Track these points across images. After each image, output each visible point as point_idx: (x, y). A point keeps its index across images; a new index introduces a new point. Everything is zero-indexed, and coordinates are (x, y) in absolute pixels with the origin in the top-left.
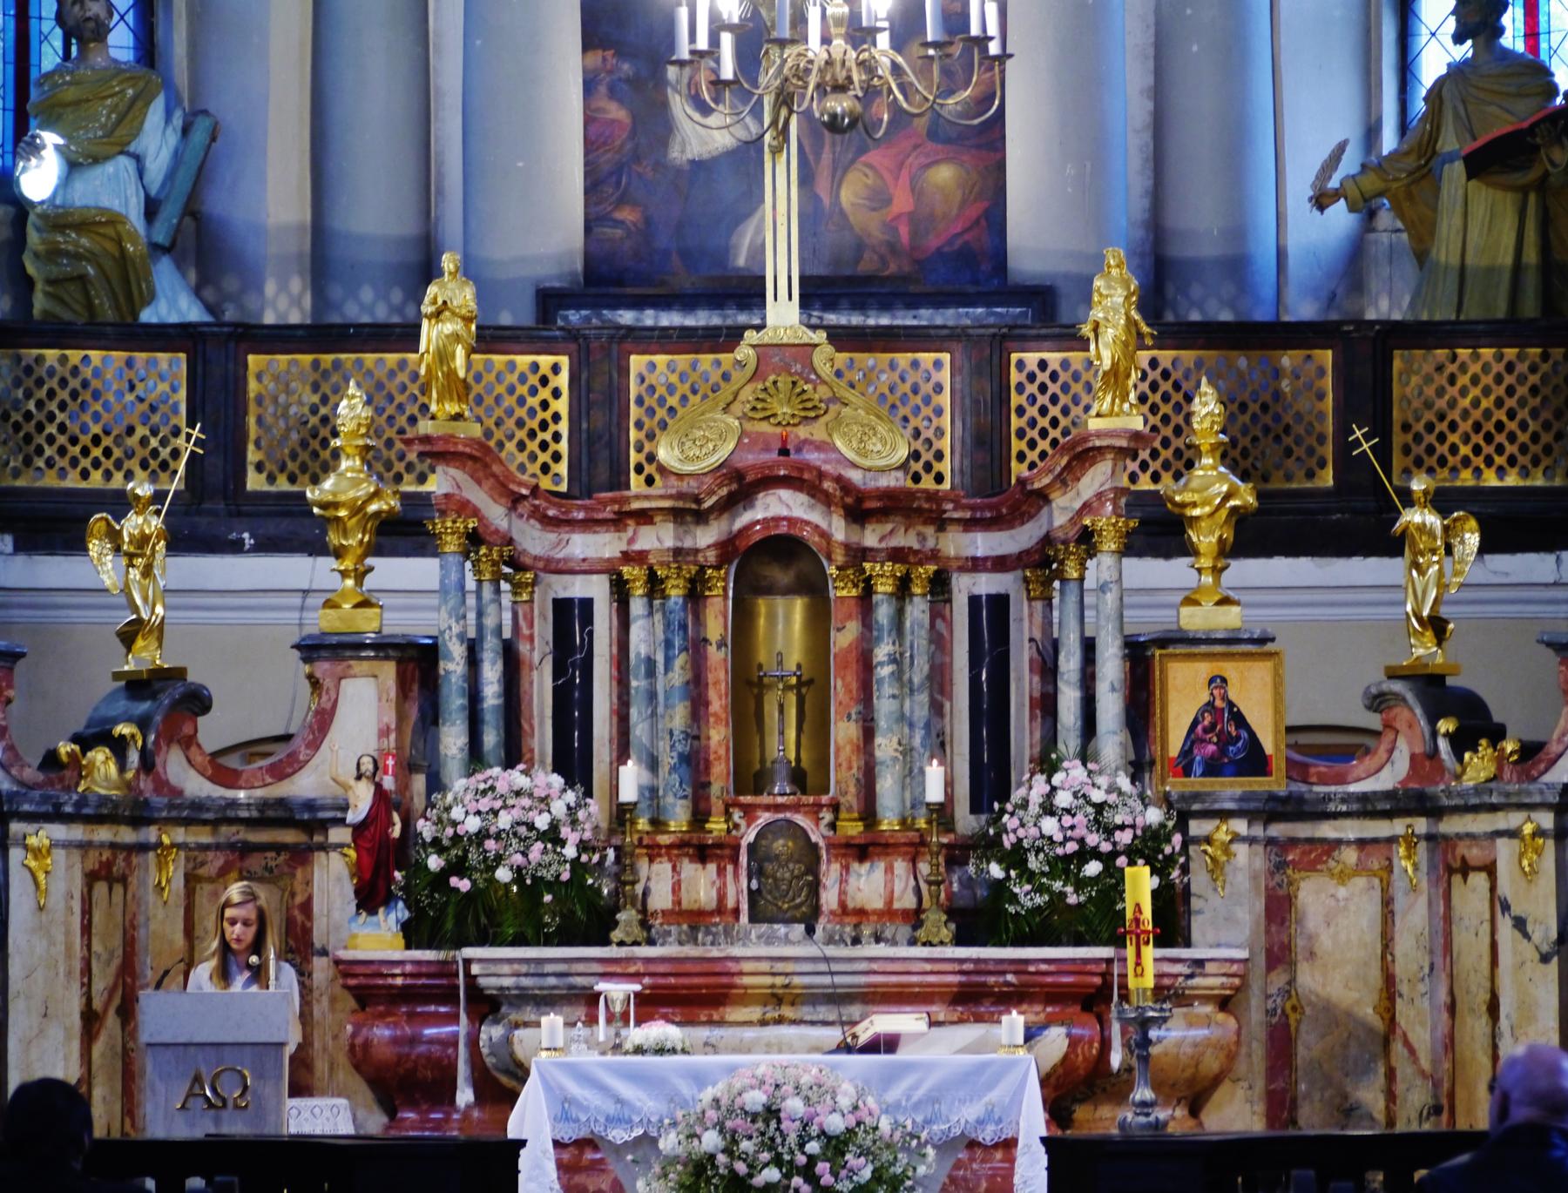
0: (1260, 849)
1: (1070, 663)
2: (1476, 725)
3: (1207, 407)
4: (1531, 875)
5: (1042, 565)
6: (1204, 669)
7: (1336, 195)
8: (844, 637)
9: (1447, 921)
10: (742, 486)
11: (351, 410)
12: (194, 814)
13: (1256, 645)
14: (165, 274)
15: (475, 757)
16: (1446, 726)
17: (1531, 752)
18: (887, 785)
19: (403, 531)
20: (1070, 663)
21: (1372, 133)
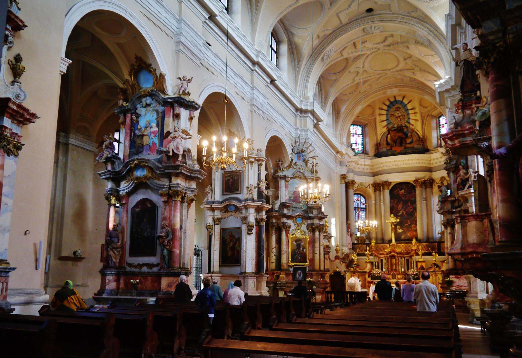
3: (420, 247)
5: (411, 257)
10: (390, 252)
12: (358, 272)
13: (424, 262)
14: (367, 240)
15: (376, 268)
17: (440, 268)
19: (371, 255)
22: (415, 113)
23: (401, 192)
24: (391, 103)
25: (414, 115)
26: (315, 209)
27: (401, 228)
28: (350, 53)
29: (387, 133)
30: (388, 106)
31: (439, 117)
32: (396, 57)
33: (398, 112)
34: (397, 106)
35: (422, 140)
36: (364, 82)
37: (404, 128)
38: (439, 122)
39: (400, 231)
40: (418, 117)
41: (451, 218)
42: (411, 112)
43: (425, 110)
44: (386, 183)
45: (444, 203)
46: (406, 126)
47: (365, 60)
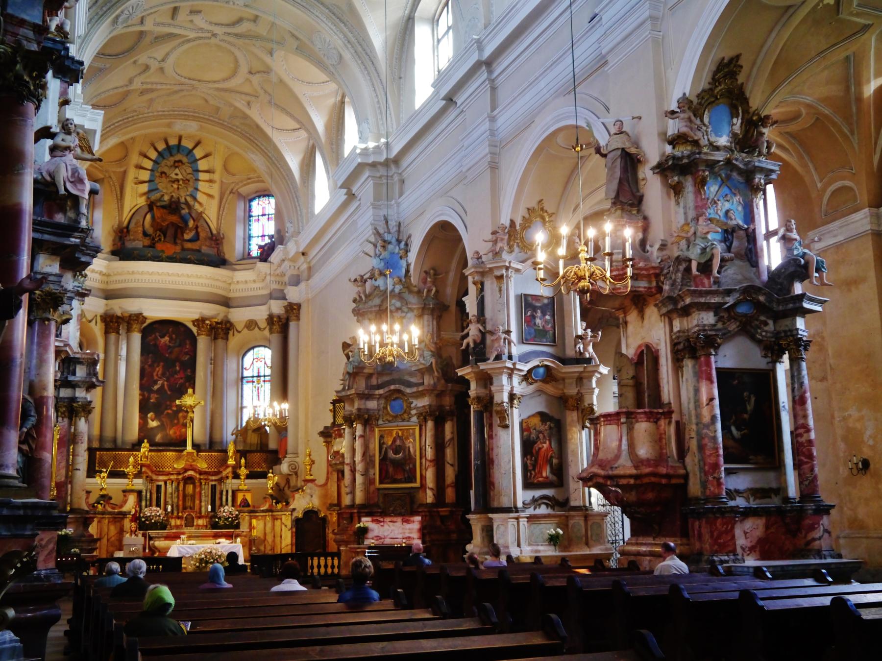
1: (224, 493)
3: (243, 461)
5: (221, 481)
8: (198, 490)
9: (274, 526)
10: (186, 470)
11: (131, 460)
12: (110, 513)
13: (248, 491)
18: (203, 509)
19: (138, 475)
20: (224, 493)
22: (210, 181)
23: (163, 340)
24: (169, 148)
25: (207, 184)
26: (81, 363)
27: (157, 417)
28: (159, 24)
29: (146, 209)
30: (160, 154)
31: (251, 200)
32: (236, 61)
33: (177, 171)
34: (178, 157)
35: (217, 240)
36: (143, 93)
37: (183, 206)
38: (250, 210)
39: (153, 424)
40: (215, 190)
42: (202, 176)
43: (228, 179)
44: (138, 317)
45: (354, 378)
46: (187, 203)
47: (175, 48)
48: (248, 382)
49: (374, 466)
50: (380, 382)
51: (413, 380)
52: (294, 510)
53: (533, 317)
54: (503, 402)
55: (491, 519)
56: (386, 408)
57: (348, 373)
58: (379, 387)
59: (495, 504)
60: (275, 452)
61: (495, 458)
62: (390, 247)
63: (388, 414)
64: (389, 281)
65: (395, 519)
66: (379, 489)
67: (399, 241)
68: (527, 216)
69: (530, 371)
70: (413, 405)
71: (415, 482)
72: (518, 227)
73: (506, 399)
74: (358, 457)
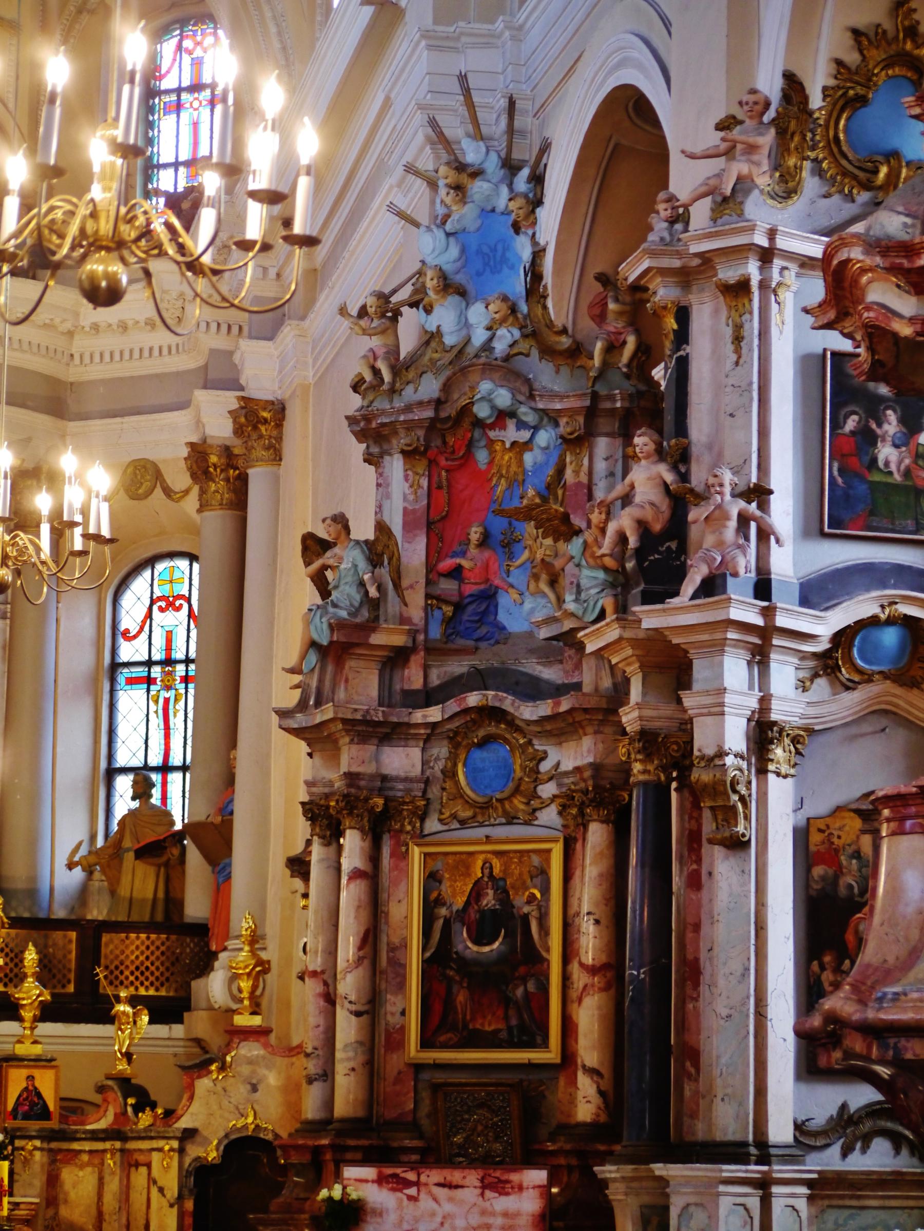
0: (45, 1153)
2: (144, 1102)
3: (31, 956)
4: (167, 1169)
6: (24, 1072)
7: (77, 864)
16: (131, 1101)
17: (169, 1114)
21: (93, 837)
41: (369, 769)
45: (339, 664)
48: (131, 681)
49: (401, 986)
50: (435, 680)
51: (550, 674)
52: (189, 1134)
53: (868, 438)
54: (721, 754)
55: (663, 1182)
56: (454, 774)
57: (314, 644)
58: (428, 697)
59: (700, 1132)
60: (201, 930)
61: (703, 955)
62: (479, 188)
63: (459, 795)
64: (478, 315)
65: (456, 1176)
66: (418, 1068)
67: (511, 167)
68: (852, 58)
69: (843, 638)
70: (545, 766)
71: (545, 1044)
72: (816, 101)
73: (735, 735)
74: (347, 949)
